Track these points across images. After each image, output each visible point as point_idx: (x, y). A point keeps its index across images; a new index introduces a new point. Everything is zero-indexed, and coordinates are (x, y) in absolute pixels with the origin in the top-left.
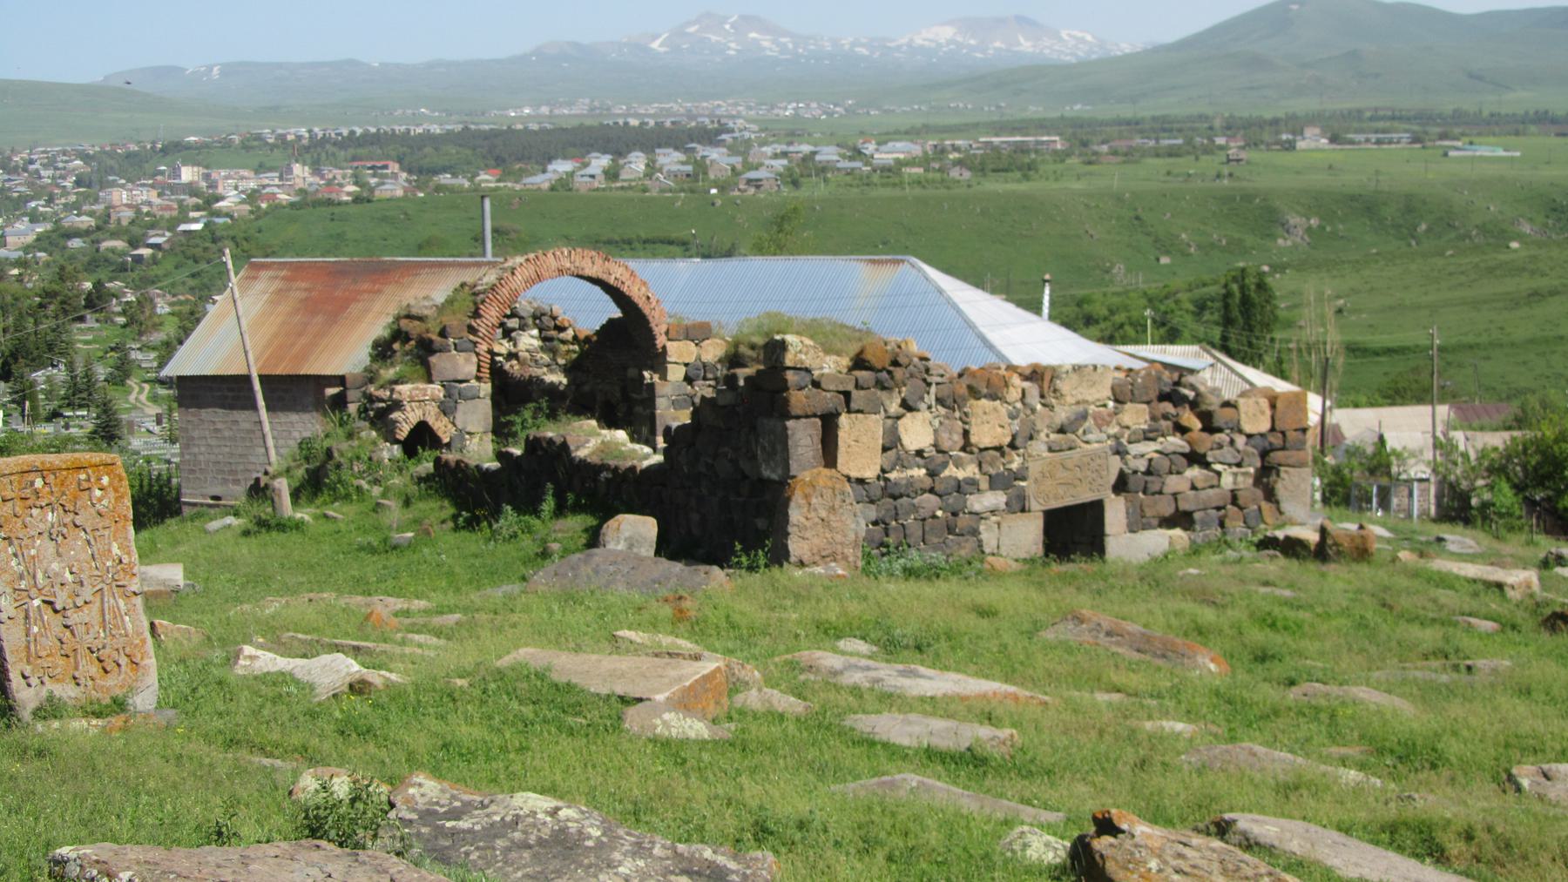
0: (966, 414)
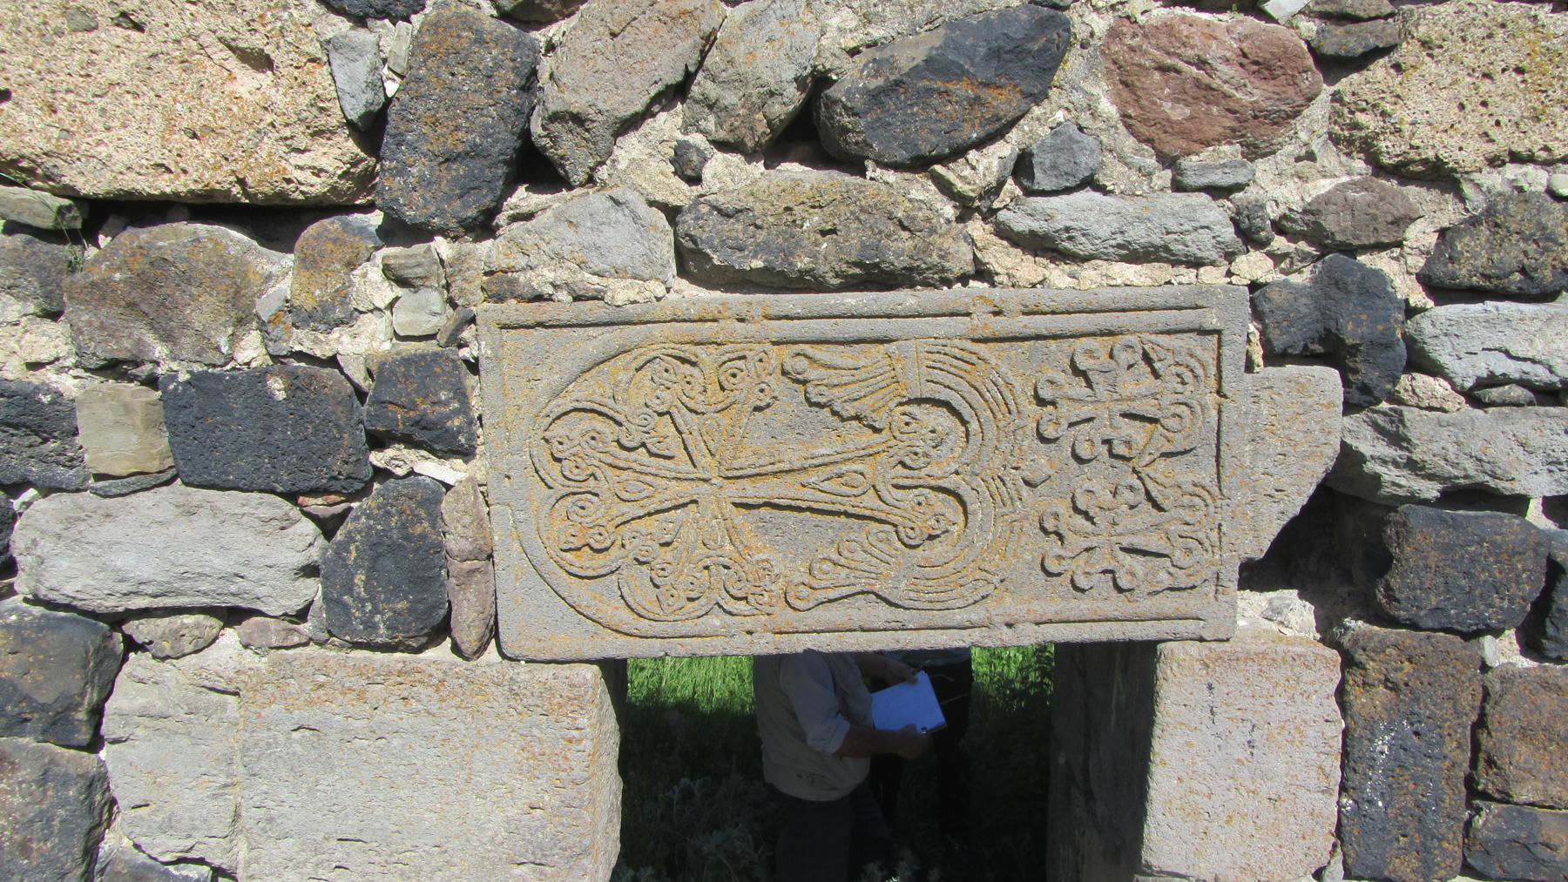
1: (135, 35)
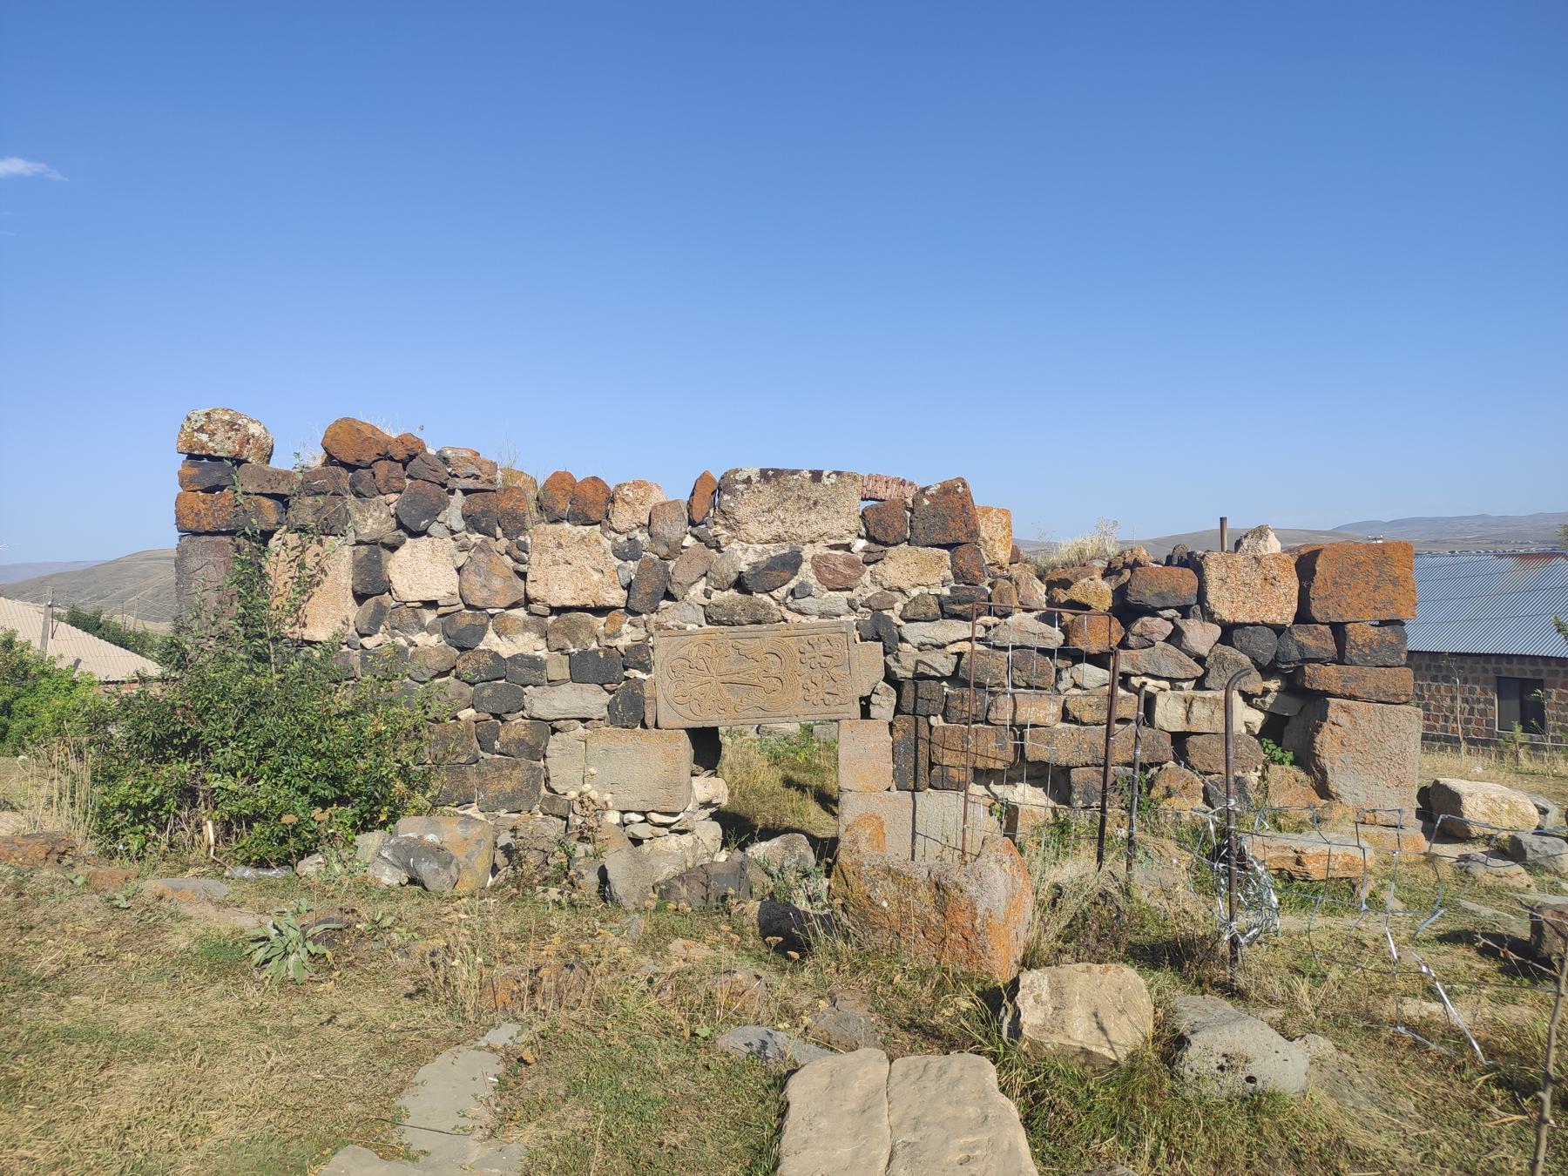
0: (523, 547)
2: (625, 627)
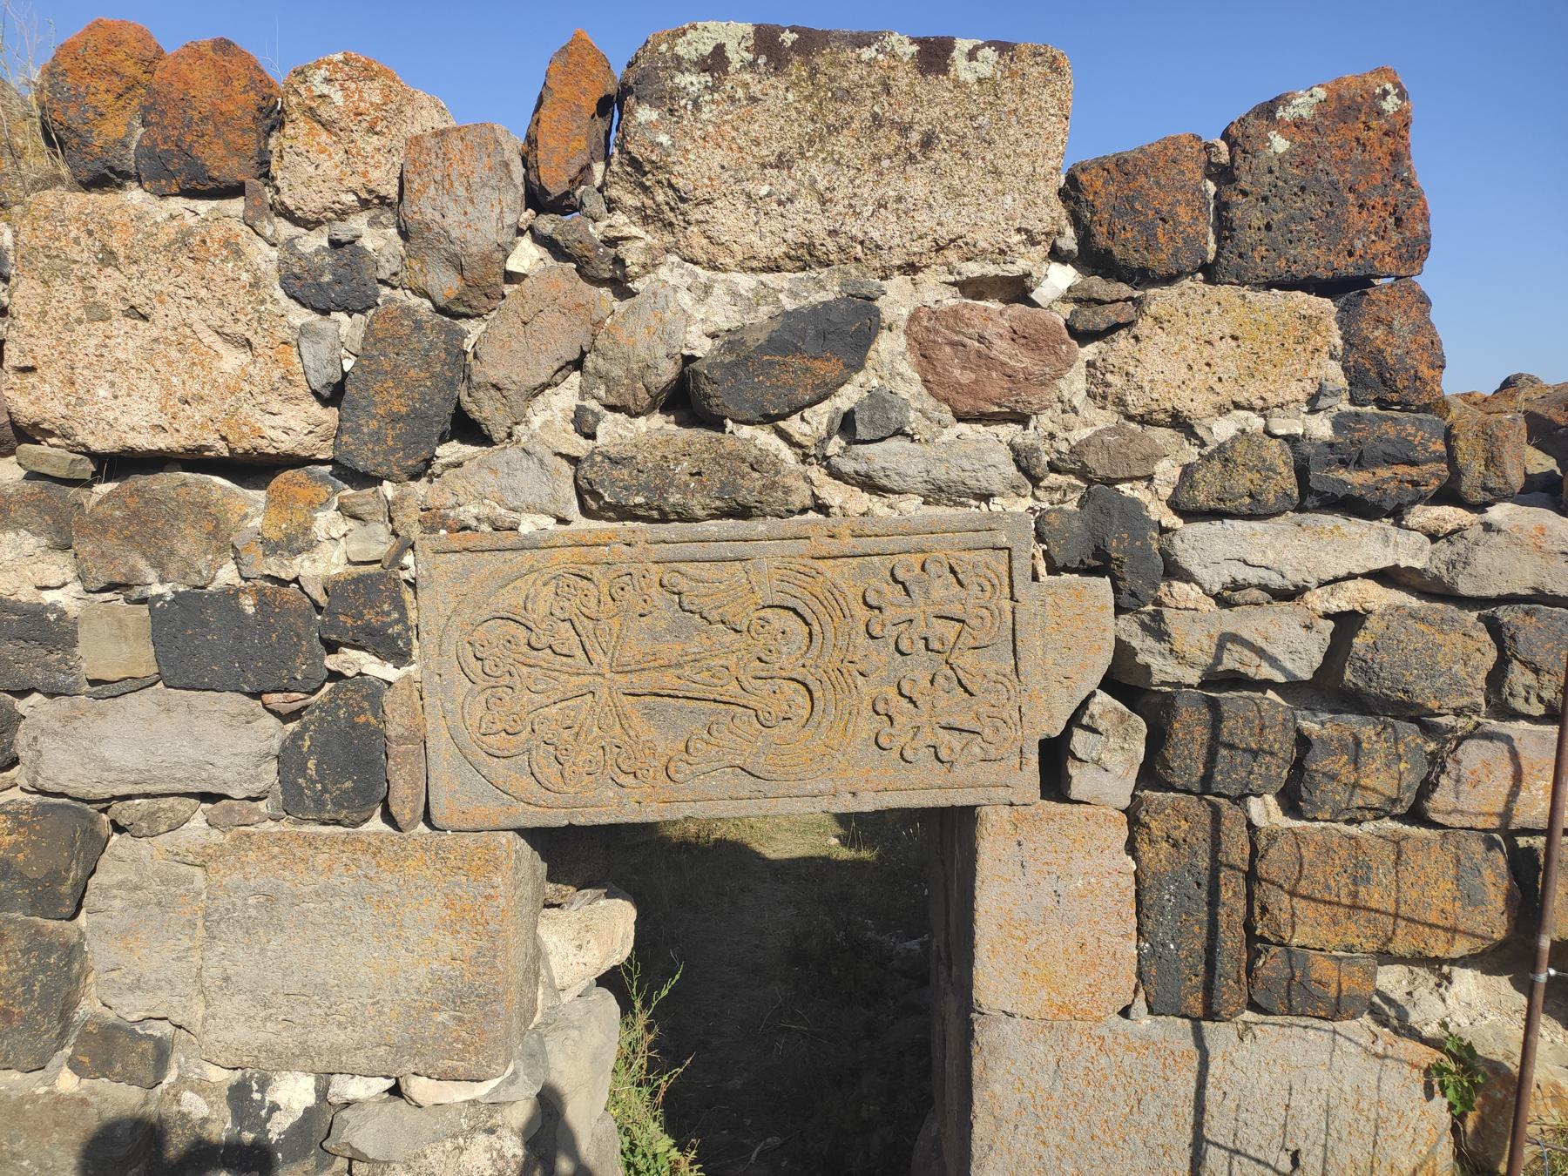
1: (141, 324)
2: (327, 522)
